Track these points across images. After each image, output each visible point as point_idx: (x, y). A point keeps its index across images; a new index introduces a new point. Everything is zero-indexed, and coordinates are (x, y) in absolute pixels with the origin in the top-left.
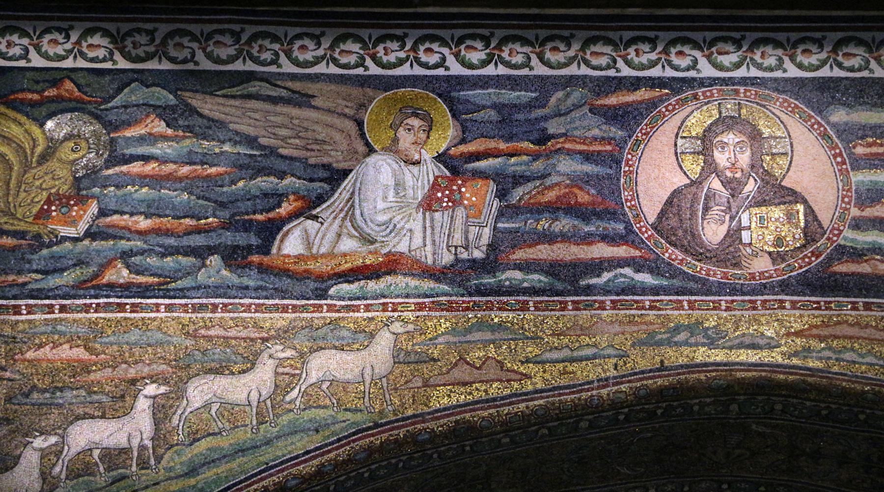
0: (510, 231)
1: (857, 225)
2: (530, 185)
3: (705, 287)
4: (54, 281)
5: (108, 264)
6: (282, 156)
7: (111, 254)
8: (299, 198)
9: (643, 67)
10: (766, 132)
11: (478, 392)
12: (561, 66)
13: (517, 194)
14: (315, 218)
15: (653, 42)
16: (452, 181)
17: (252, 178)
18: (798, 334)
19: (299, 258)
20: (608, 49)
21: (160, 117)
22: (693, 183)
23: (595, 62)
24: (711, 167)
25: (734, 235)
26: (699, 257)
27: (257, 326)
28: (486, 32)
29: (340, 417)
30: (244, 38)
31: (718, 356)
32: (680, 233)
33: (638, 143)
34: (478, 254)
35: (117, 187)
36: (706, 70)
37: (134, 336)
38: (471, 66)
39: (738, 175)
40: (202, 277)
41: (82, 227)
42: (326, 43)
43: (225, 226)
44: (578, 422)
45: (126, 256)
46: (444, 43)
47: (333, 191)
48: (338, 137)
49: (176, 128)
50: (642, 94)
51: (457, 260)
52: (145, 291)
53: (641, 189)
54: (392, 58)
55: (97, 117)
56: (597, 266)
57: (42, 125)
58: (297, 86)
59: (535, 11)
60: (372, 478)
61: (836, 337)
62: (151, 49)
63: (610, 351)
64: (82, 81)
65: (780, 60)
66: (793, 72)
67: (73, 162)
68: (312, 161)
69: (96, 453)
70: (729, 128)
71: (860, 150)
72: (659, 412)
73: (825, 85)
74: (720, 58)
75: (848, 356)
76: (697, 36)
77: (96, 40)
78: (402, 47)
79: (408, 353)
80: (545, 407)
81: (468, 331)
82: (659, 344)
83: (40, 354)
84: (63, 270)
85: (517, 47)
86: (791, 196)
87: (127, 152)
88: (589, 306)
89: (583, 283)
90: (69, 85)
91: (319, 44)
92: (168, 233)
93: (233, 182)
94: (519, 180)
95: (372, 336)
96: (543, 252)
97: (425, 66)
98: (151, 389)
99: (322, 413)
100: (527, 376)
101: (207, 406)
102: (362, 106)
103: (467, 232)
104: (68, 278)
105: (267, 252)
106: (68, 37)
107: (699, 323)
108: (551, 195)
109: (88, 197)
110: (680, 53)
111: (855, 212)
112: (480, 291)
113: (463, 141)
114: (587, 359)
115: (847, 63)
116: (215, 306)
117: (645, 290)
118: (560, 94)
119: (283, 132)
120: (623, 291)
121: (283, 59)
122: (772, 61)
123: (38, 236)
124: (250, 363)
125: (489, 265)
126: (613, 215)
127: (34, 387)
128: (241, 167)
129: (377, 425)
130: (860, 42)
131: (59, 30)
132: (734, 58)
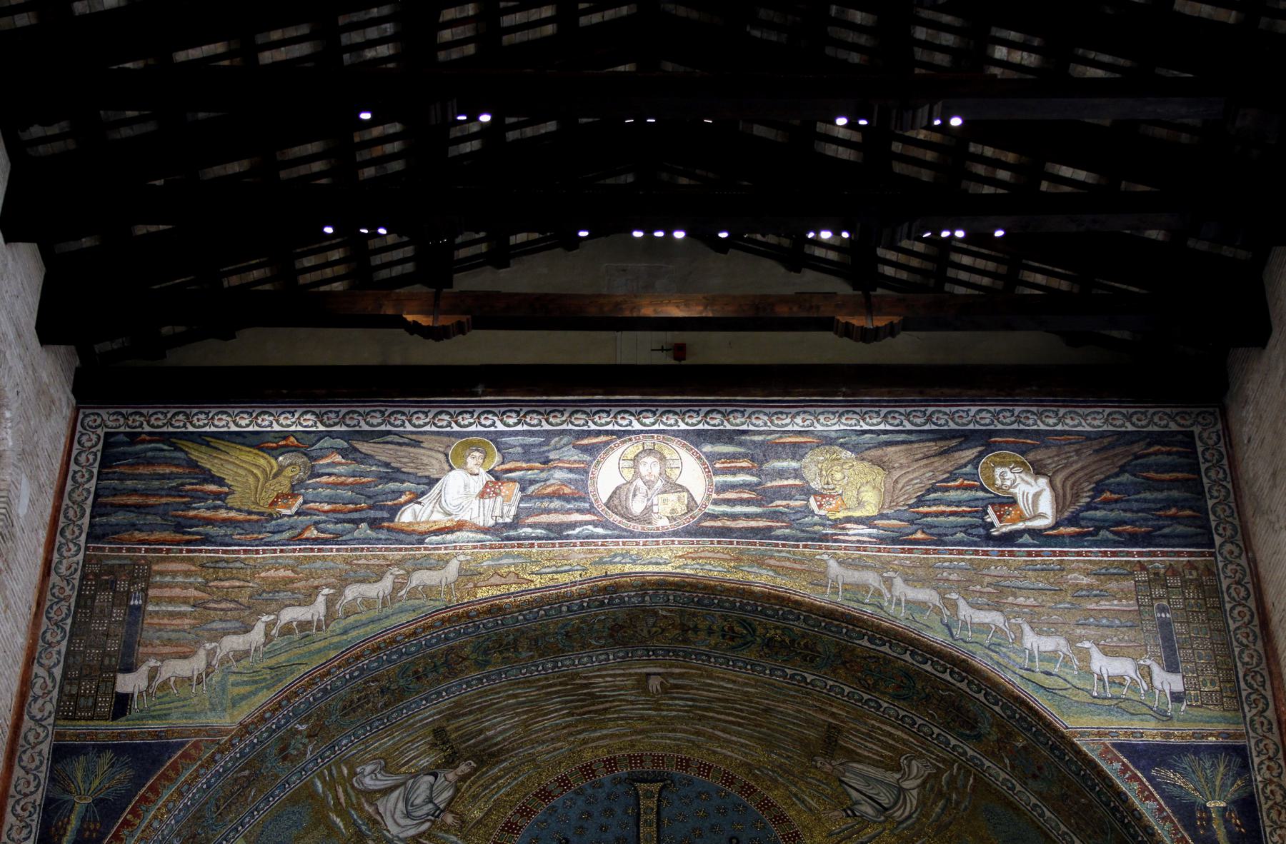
0: (526, 508)
1: (716, 502)
2: (538, 485)
3: (633, 535)
4: (276, 537)
5: (307, 528)
6: (404, 473)
7: (308, 523)
8: (411, 492)
9: (602, 425)
10: (668, 457)
11: (504, 590)
12: (558, 425)
13: (531, 490)
14: (420, 503)
15: (608, 413)
16: (496, 483)
17: (387, 483)
18: (680, 557)
19: (410, 524)
20: (584, 416)
21: (339, 454)
22: (628, 483)
23: (576, 423)
24: (637, 474)
25: (648, 509)
26: (629, 519)
27: (385, 558)
28: (518, 409)
29: (427, 604)
30: (387, 414)
31: (638, 569)
32: (620, 508)
33: (598, 463)
34: (508, 520)
35: (314, 489)
36: (637, 426)
37: (318, 564)
38: (509, 426)
39: (653, 478)
40: (356, 534)
41: (294, 509)
42: (431, 415)
43: (370, 508)
44: (560, 607)
45: (316, 524)
46: (495, 414)
47: (430, 489)
48: (434, 462)
49: (347, 459)
50: (602, 438)
51: (497, 524)
52: (325, 541)
53: (599, 486)
54: (466, 422)
55: (305, 454)
56: (573, 525)
57: (276, 459)
58: (414, 437)
59: (545, 398)
60: (447, 639)
61: (701, 558)
62: (337, 420)
63: (579, 568)
64: (299, 437)
65: (677, 421)
66: (683, 427)
67: (292, 477)
68: (420, 474)
69: (295, 624)
70: (649, 455)
71: (718, 465)
72: (606, 601)
73: (700, 433)
74: (644, 420)
75: (707, 567)
76: (632, 410)
77: (308, 416)
78: (472, 417)
79: (466, 570)
80: (541, 597)
81: (501, 559)
82: (605, 563)
83: (268, 574)
84: (282, 532)
85: (534, 416)
86: (682, 488)
87: (321, 471)
88: (568, 545)
89: (565, 533)
90: (292, 439)
91: (427, 416)
92: (340, 512)
93: (376, 486)
94: (532, 482)
95: (447, 562)
96: (544, 518)
97: (484, 426)
98: (326, 591)
99: (417, 602)
100: (532, 581)
101: (355, 599)
102: (449, 446)
103: (502, 509)
104: (286, 535)
105: (393, 521)
106: (293, 416)
107: (628, 552)
108: (549, 490)
109: (298, 495)
110: (623, 418)
111: (714, 496)
112: (508, 538)
113: (503, 463)
114: (565, 571)
115: (712, 422)
116: (362, 549)
117: (599, 537)
118: (557, 439)
119: (405, 460)
120: (587, 537)
121: (407, 424)
122: (672, 422)
123: (271, 515)
124: (380, 578)
125: (515, 524)
126: (583, 499)
127: (264, 591)
128: (381, 478)
129: (447, 608)
130: (719, 412)
131: (289, 412)
132: (652, 420)
